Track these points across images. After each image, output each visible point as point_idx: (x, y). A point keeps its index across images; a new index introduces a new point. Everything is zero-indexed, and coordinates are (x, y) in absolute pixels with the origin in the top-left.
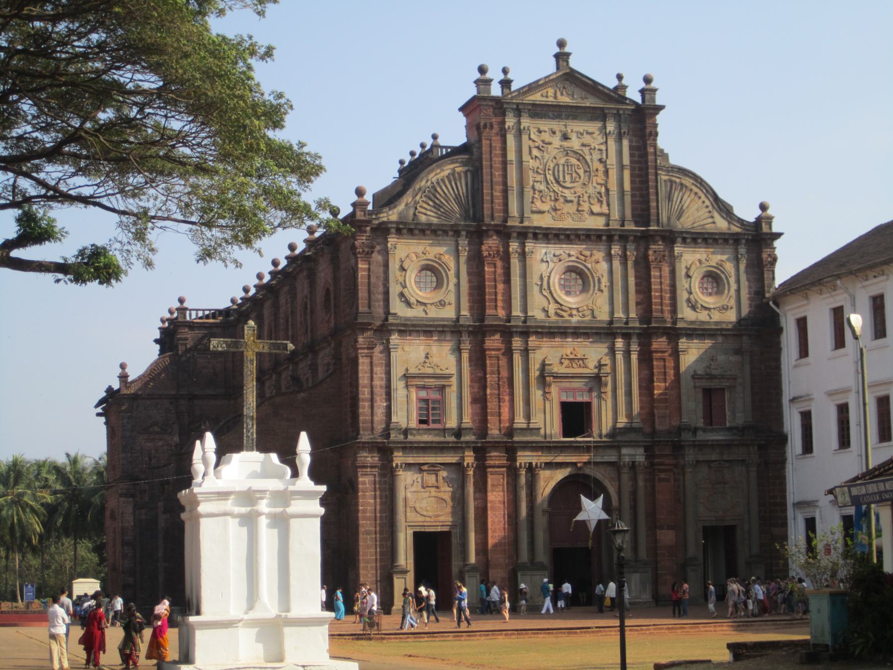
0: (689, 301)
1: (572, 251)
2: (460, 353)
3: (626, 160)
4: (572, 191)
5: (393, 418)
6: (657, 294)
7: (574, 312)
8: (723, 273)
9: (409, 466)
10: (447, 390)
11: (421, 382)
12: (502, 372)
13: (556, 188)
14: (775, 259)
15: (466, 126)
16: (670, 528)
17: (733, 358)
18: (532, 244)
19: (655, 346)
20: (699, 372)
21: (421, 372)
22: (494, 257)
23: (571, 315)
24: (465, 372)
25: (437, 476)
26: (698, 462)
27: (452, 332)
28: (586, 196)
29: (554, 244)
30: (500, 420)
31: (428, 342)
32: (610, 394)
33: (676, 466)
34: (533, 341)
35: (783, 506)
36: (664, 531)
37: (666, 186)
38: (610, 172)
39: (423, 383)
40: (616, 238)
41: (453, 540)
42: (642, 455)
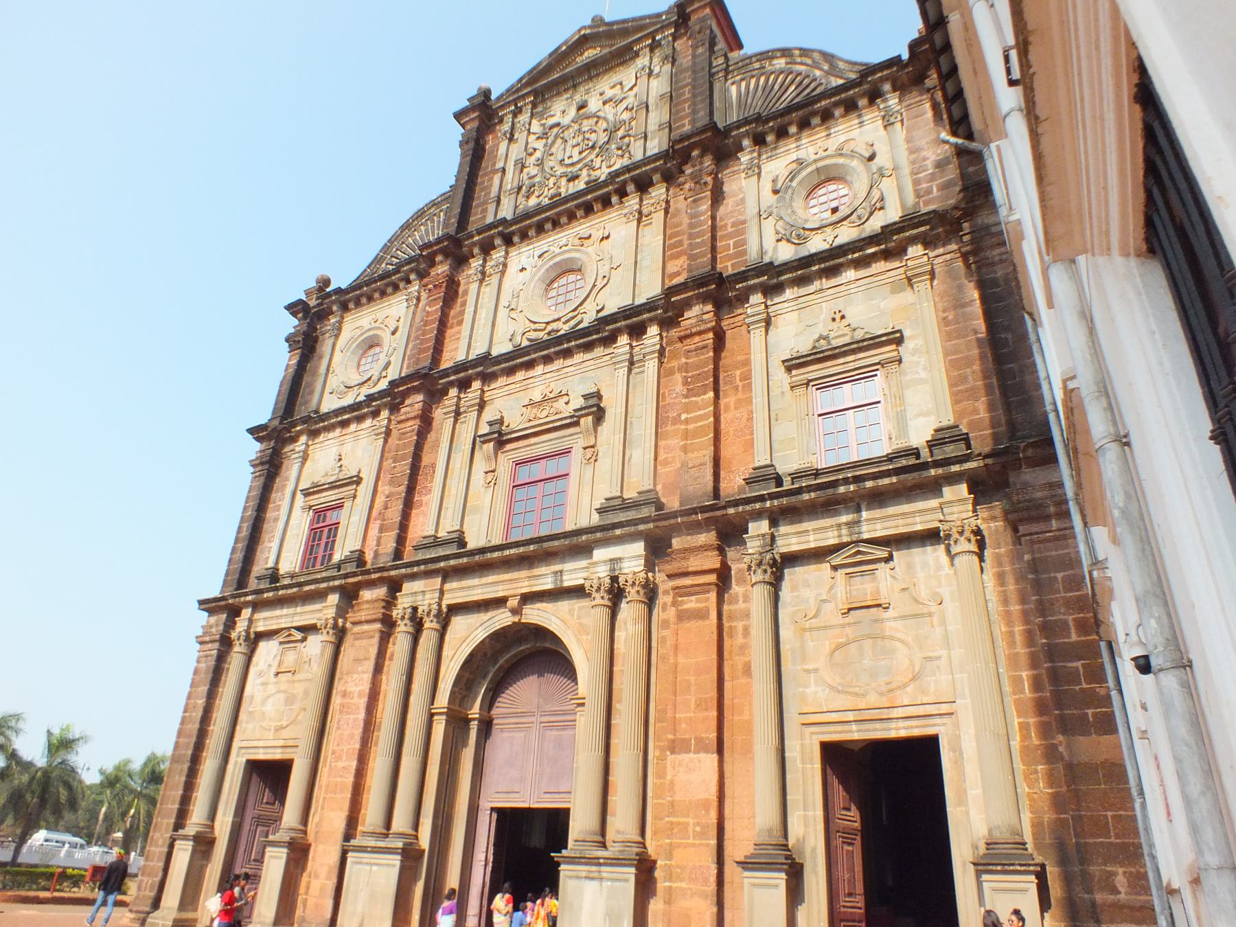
7: (554, 326)
13: (560, 170)
23: (549, 334)
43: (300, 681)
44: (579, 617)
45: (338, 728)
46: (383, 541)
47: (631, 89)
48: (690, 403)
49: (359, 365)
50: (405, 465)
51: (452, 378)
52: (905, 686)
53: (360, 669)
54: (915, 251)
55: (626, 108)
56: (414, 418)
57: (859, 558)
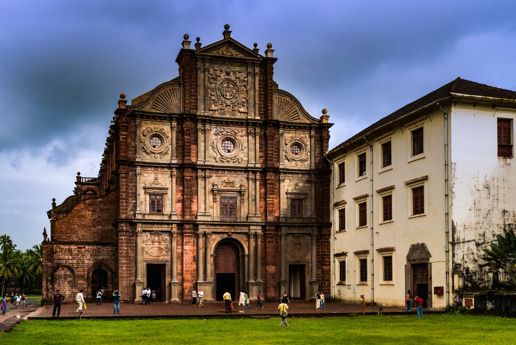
0: (286, 156)
1: (228, 130)
2: (172, 178)
4: (230, 101)
5: (137, 208)
7: (229, 160)
8: (303, 143)
9: (144, 231)
10: (165, 196)
11: (151, 191)
12: (192, 188)
14: (329, 137)
15: (179, 69)
16: (273, 265)
17: (306, 185)
18: (209, 126)
19: (268, 177)
20: (290, 191)
21: (152, 186)
23: (228, 161)
25: (159, 237)
26: (287, 234)
27: (168, 168)
28: (236, 104)
29: (220, 126)
30: (191, 212)
31: (156, 172)
32: (246, 201)
33: (277, 235)
34: (208, 173)
35: (329, 255)
36: (270, 266)
38: (249, 91)
39: (153, 192)
41: (166, 268)
42: (260, 229)
43: (162, 245)
49: (150, 142)
52: (302, 257)
54: (312, 175)
55: (244, 85)
57: (298, 236)
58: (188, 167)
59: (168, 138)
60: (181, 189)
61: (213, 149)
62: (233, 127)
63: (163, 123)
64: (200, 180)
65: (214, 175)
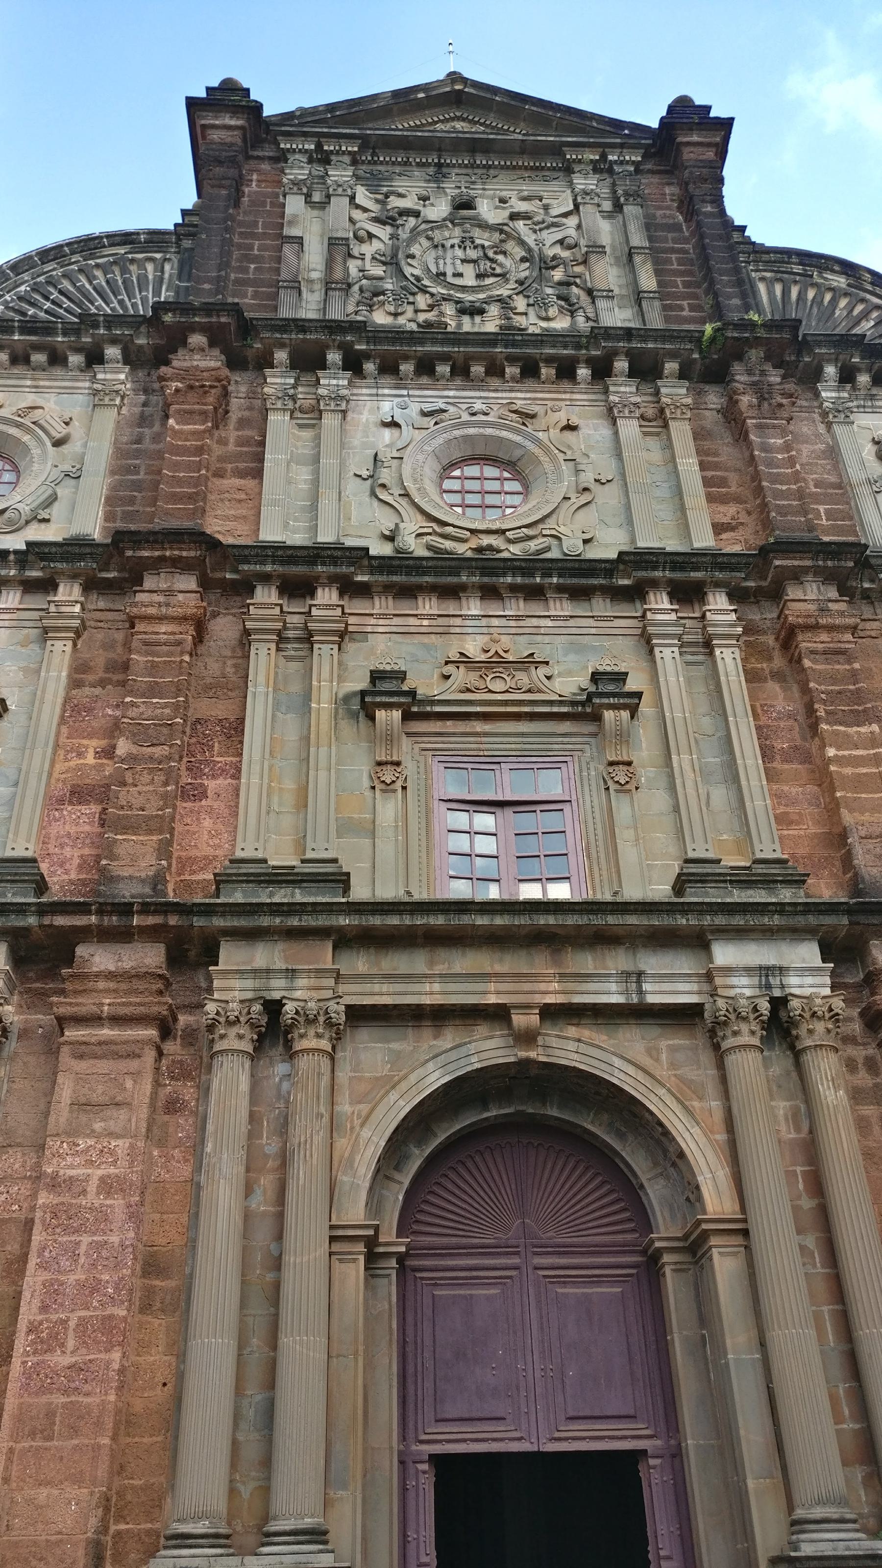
3: (638, 239)
6: (784, 488)
22: (205, 393)
23: (479, 550)
24: (49, 697)
27: (30, 587)
37: (771, 293)
38: (593, 258)
40: (621, 365)
42: (814, 971)
44: (673, 1065)
45: (39, 1266)
46: (120, 850)
47: (566, 215)
48: (836, 733)
50: (166, 705)
51: (269, 568)
53: (98, 1126)
55: (561, 242)
56: (183, 619)
58: (163, 559)
59: (65, 449)
60: (110, 712)
61: (377, 497)
62: (511, 391)
63: (42, 383)
64: (263, 652)
65: (383, 625)
